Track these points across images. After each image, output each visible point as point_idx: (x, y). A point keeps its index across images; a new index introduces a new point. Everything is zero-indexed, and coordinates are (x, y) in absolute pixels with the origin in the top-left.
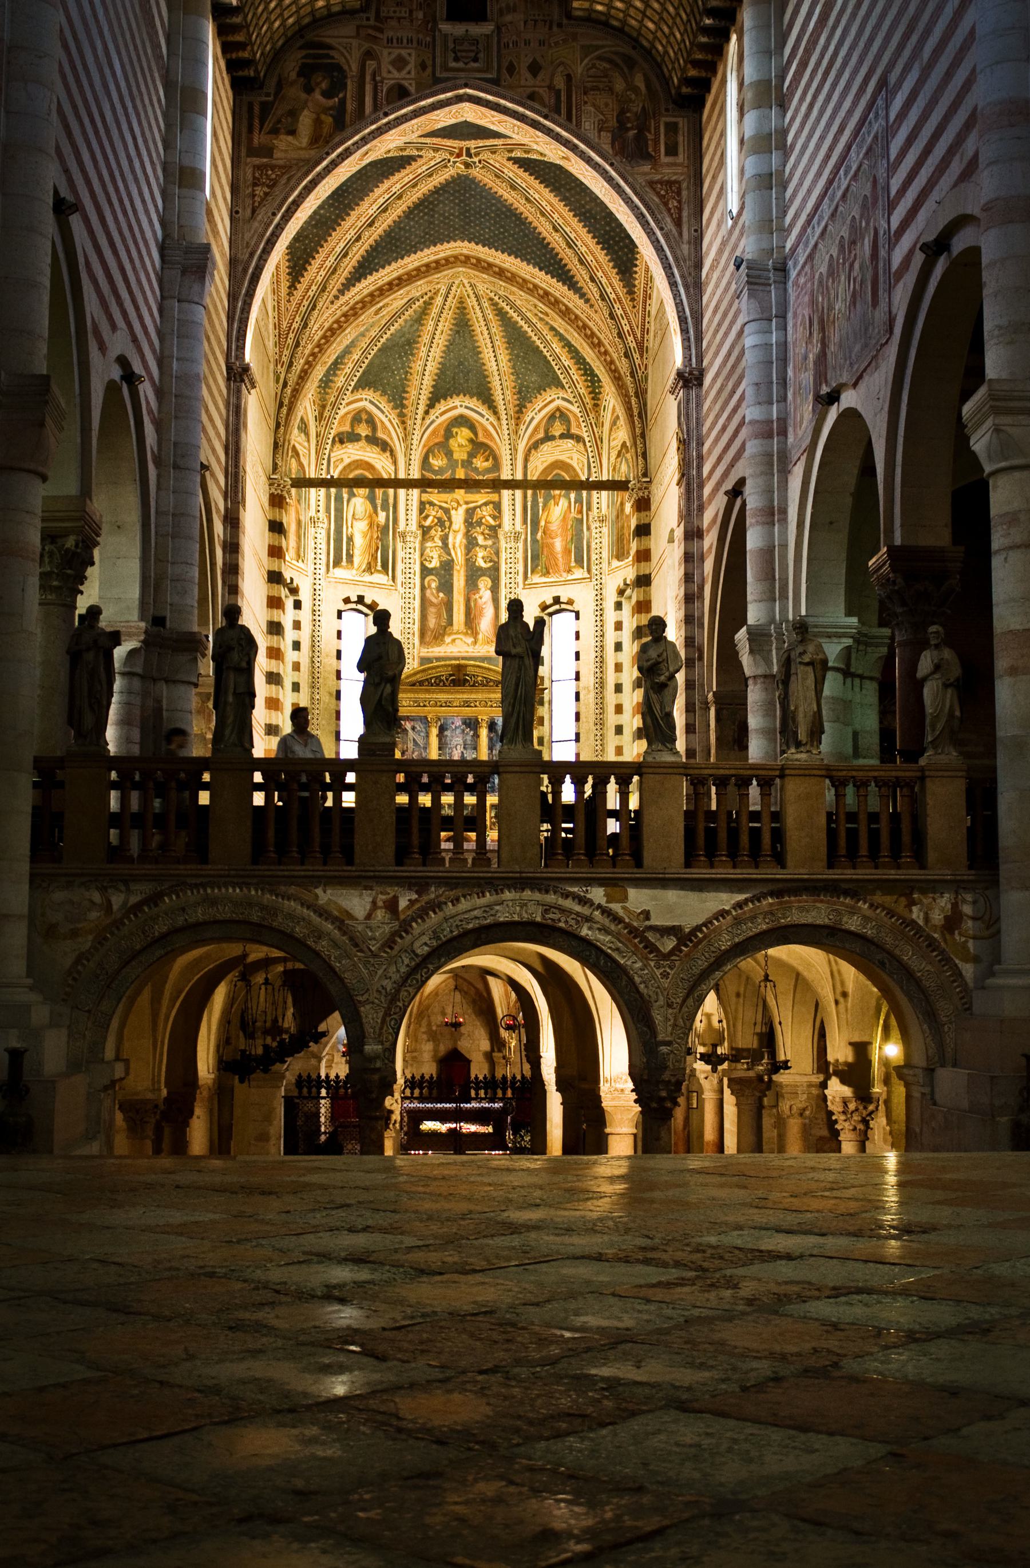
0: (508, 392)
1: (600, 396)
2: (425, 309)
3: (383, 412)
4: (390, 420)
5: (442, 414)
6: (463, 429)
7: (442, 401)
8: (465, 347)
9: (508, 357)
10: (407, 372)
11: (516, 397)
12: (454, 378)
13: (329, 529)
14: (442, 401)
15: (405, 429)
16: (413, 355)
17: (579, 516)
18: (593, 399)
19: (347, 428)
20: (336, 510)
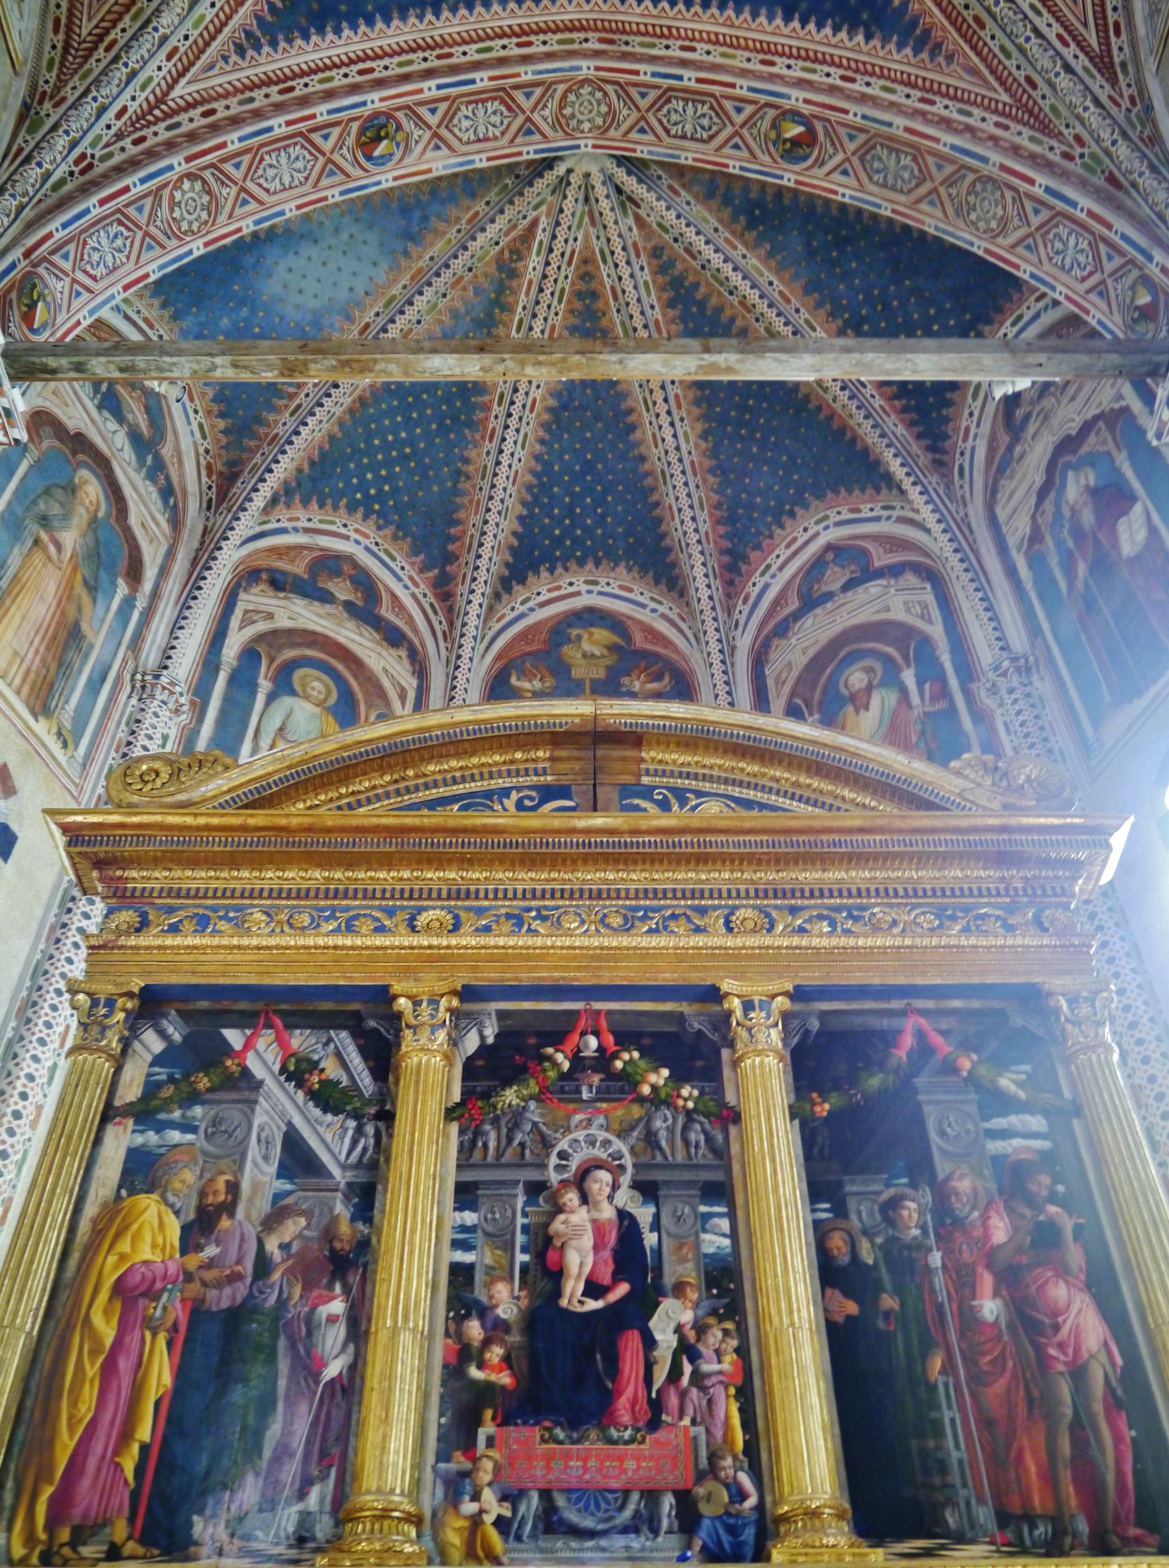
0: (703, 516)
1: (947, 444)
2: (501, 289)
3: (399, 579)
4: (414, 596)
5: (542, 605)
6: (594, 630)
7: (545, 574)
8: (598, 418)
9: (699, 426)
10: (459, 473)
11: (722, 530)
12: (570, 509)
13: (196, 731)
14: (545, 574)
15: (450, 610)
16: (470, 424)
17: (942, 705)
18: (932, 449)
19: (299, 568)
20: (227, 699)
